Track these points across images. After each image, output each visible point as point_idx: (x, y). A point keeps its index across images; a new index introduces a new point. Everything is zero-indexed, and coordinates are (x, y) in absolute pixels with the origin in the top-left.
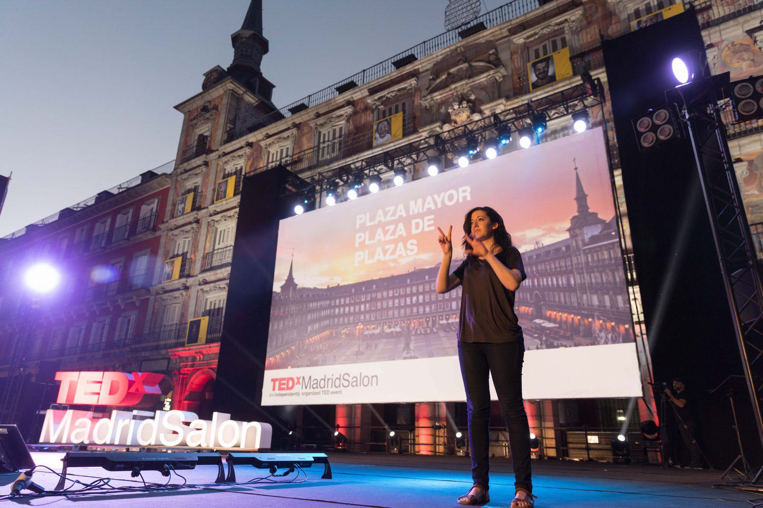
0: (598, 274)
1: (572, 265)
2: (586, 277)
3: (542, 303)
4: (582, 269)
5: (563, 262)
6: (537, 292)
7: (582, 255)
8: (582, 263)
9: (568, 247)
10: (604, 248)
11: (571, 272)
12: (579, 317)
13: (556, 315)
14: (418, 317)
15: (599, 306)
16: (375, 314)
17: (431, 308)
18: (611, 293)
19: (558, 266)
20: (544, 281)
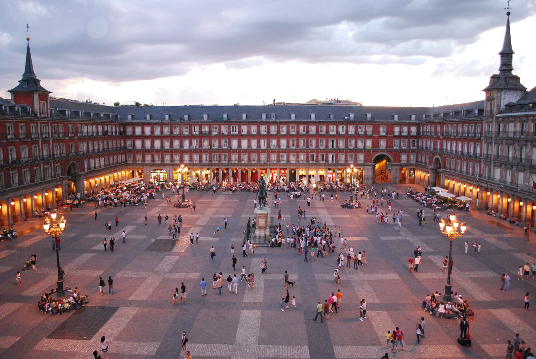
0: (506, 147)
1: (481, 133)
2: (493, 147)
3: (442, 169)
4: (491, 138)
5: (473, 128)
6: (438, 156)
7: (494, 122)
8: (492, 132)
9: (481, 111)
10: (518, 120)
11: (479, 140)
12: (478, 190)
13: (454, 185)
14: (277, 167)
15: (500, 181)
16: (208, 155)
17: (298, 157)
18: (514, 169)
19: (466, 130)
20: (448, 146)
